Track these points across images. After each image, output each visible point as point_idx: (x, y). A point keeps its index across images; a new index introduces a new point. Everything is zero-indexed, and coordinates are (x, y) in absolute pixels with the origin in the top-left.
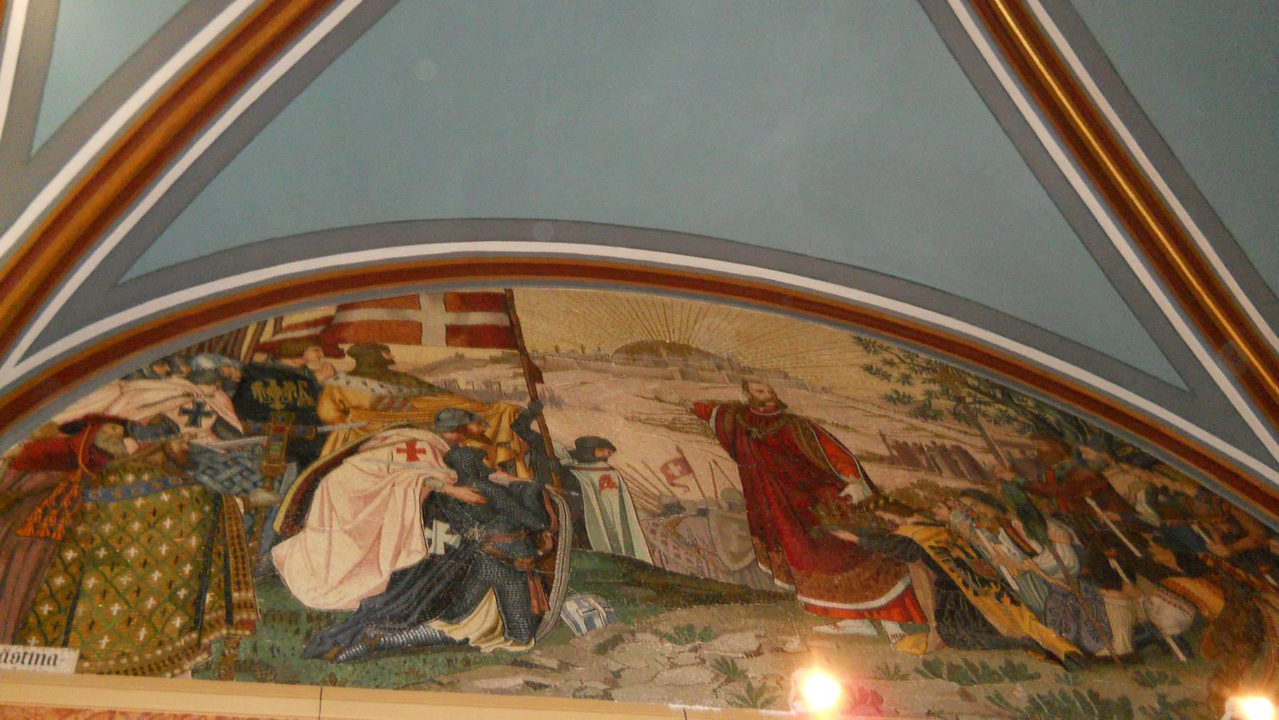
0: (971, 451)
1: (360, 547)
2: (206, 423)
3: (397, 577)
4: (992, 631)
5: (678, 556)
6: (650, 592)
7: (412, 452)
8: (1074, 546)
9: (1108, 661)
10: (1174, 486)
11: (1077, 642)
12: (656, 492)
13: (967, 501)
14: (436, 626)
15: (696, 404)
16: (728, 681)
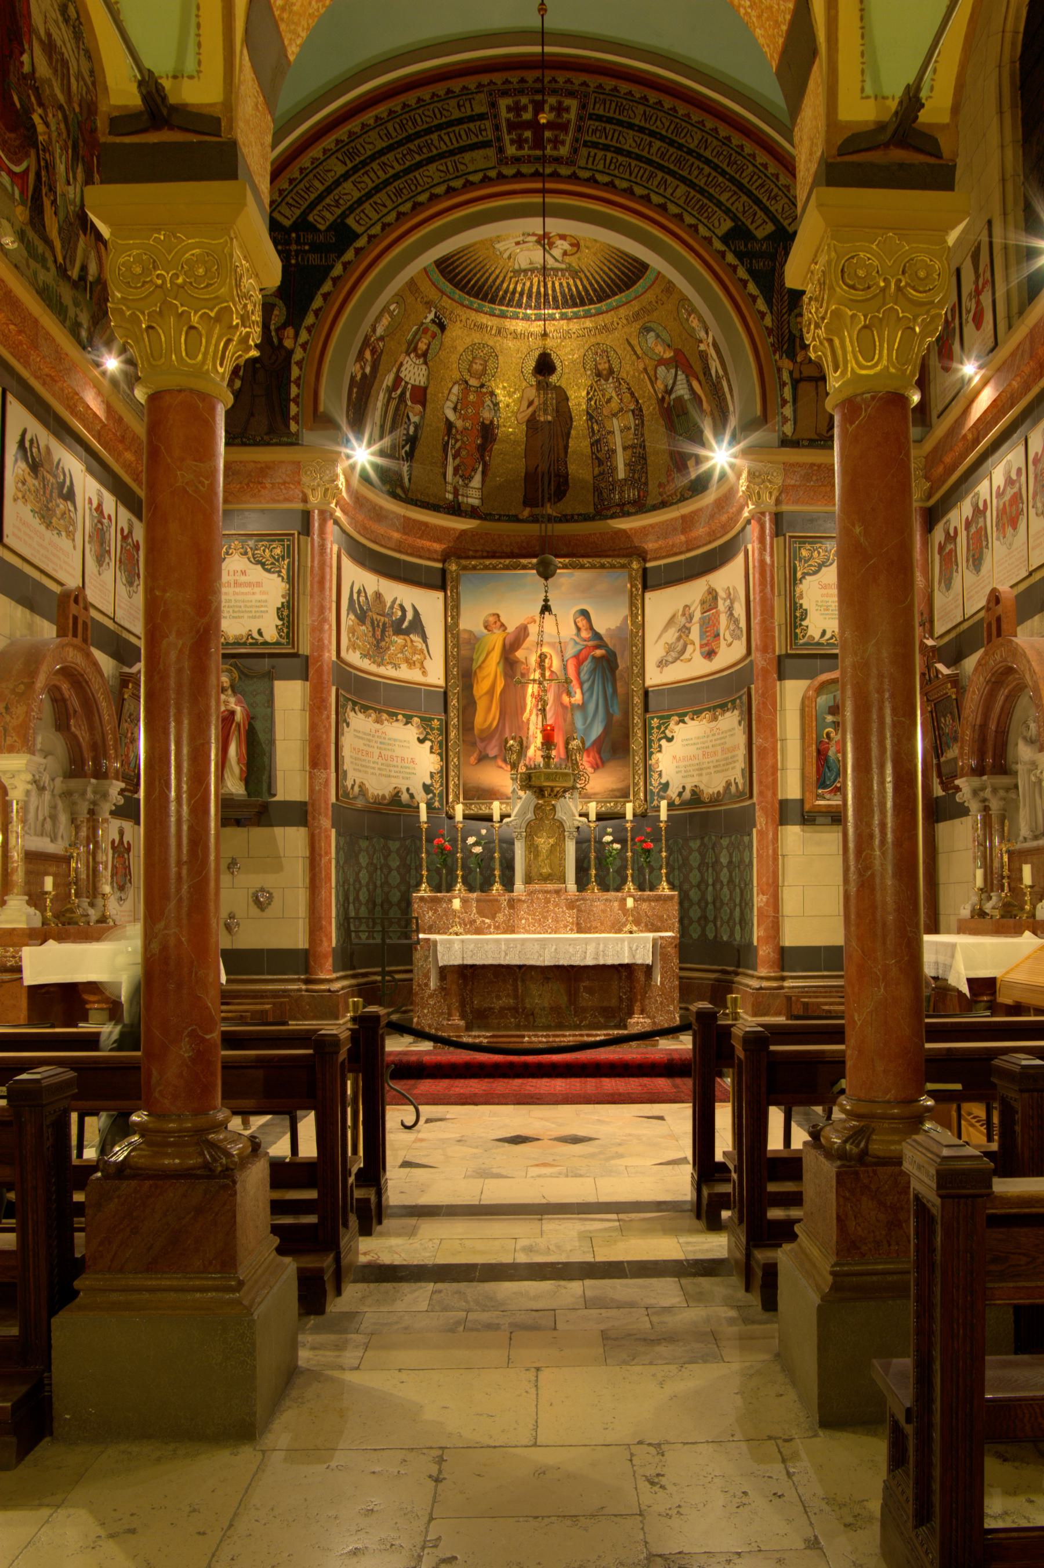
0: (71, 72)
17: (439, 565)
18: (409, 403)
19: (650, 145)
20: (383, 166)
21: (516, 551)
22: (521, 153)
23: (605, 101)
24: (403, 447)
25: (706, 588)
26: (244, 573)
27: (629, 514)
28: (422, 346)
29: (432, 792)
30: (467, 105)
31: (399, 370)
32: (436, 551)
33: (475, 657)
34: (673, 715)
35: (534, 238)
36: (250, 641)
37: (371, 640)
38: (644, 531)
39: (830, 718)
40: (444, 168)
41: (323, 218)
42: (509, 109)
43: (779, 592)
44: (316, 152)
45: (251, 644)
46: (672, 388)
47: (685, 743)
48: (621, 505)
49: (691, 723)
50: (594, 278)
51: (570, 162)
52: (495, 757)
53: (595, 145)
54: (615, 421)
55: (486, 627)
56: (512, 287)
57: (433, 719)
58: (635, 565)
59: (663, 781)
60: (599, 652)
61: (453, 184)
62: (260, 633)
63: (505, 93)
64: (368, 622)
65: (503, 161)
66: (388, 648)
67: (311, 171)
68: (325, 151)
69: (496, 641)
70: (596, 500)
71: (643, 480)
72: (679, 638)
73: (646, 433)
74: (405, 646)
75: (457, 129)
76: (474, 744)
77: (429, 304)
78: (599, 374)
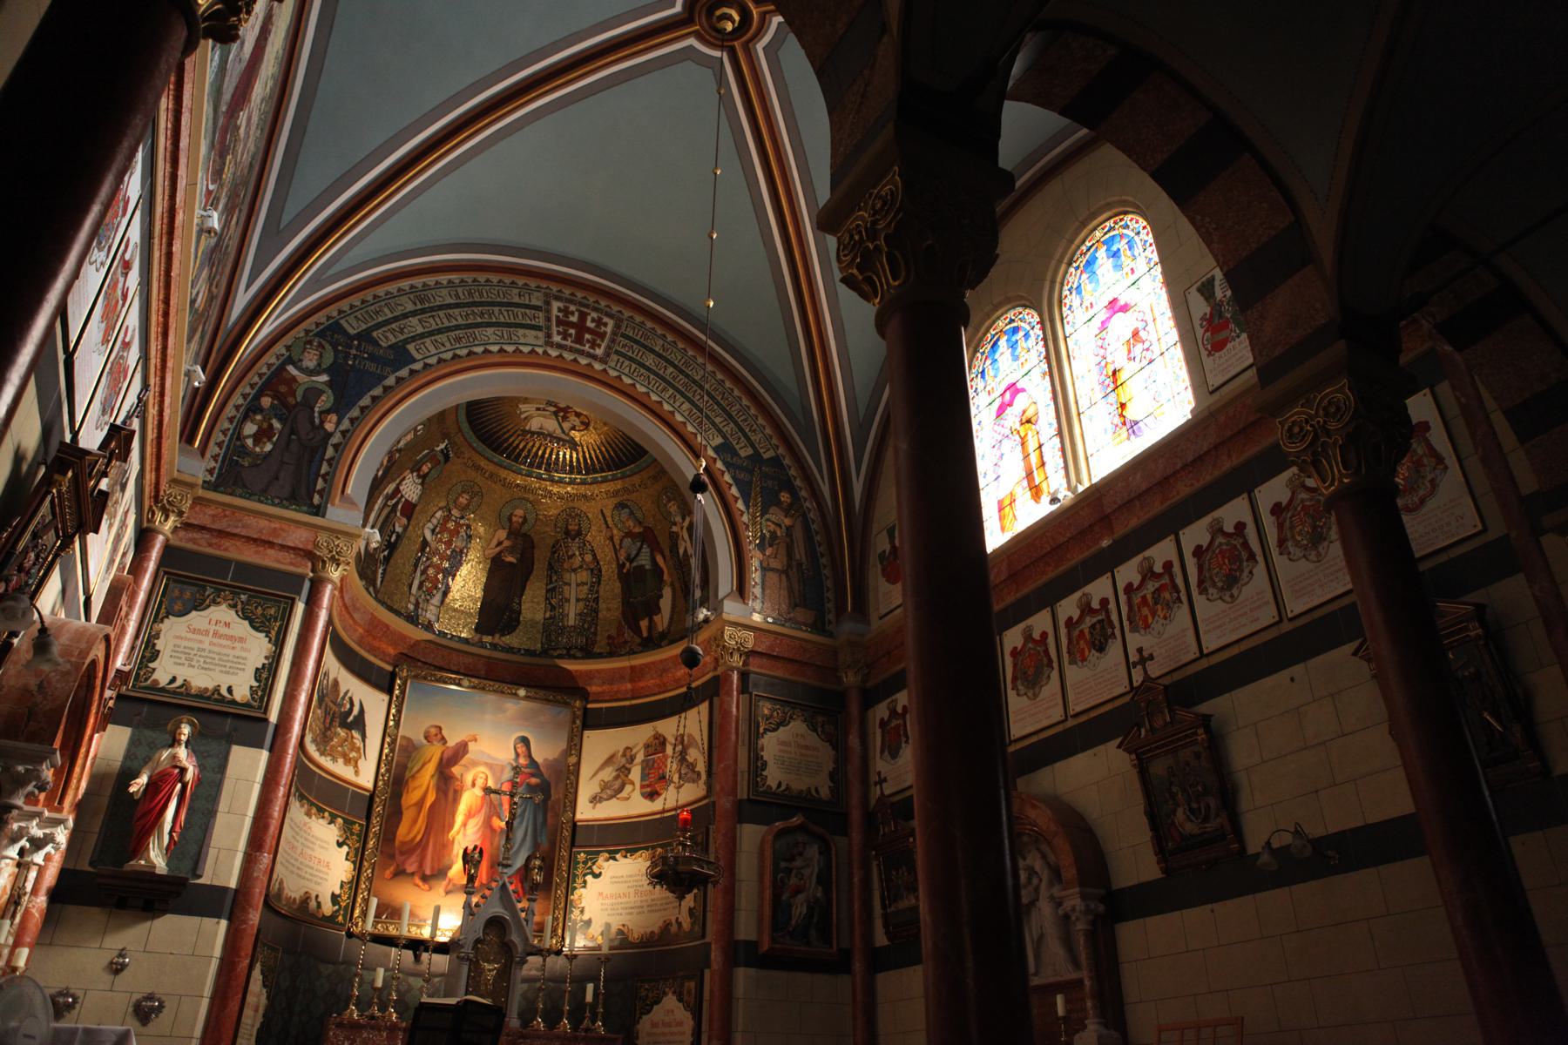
17: (390, 668)
18: (398, 514)
19: (666, 368)
20: (449, 317)
21: (462, 671)
22: (564, 342)
23: (634, 328)
24: (384, 551)
25: (653, 733)
26: (227, 625)
27: (575, 657)
28: (425, 469)
29: (339, 904)
30: (527, 296)
31: (400, 483)
32: (390, 655)
33: (409, 765)
34: (601, 852)
35: (553, 409)
36: (216, 696)
37: (322, 726)
38: (590, 675)
39: (783, 864)
40: (500, 334)
41: (386, 338)
42: (560, 310)
43: (743, 742)
44: (392, 287)
45: (216, 700)
46: (634, 558)
47: (614, 880)
48: (569, 649)
49: (623, 861)
50: (590, 454)
51: (603, 361)
52: (413, 874)
53: (624, 356)
54: (573, 574)
55: (426, 738)
56: (516, 442)
57: (354, 823)
58: (578, 704)
59: (586, 917)
60: (534, 781)
61: (505, 347)
62: (230, 690)
63: (557, 298)
64: (323, 707)
65: (549, 343)
66: (332, 739)
68: (399, 290)
69: (434, 753)
70: (544, 640)
71: (592, 630)
72: (617, 777)
73: (601, 593)
74: (346, 740)
75: (516, 310)
76: (392, 857)
77: (445, 436)
78: (567, 533)
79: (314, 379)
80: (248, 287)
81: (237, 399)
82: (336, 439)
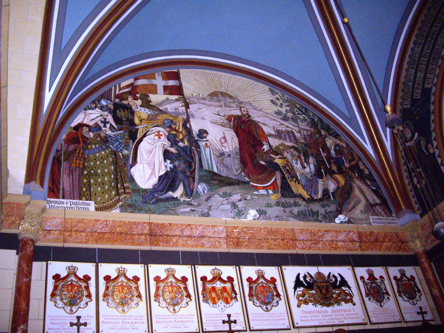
1: (151, 169)
2: (108, 126)
3: (160, 177)
4: (293, 192)
5: (223, 170)
6: (217, 182)
7: (159, 136)
8: (314, 164)
9: (316, 200)
10: (341, 144)
11: (310, 195)
12: (219, 149)
13: (292, 150)
14: (170, 193)
15: (228, 116)
16: (234, 209)
67: (406, 82)
79: (415, 139)
80: (366, 143)
81: (405, 174)
82: (437, 152)
